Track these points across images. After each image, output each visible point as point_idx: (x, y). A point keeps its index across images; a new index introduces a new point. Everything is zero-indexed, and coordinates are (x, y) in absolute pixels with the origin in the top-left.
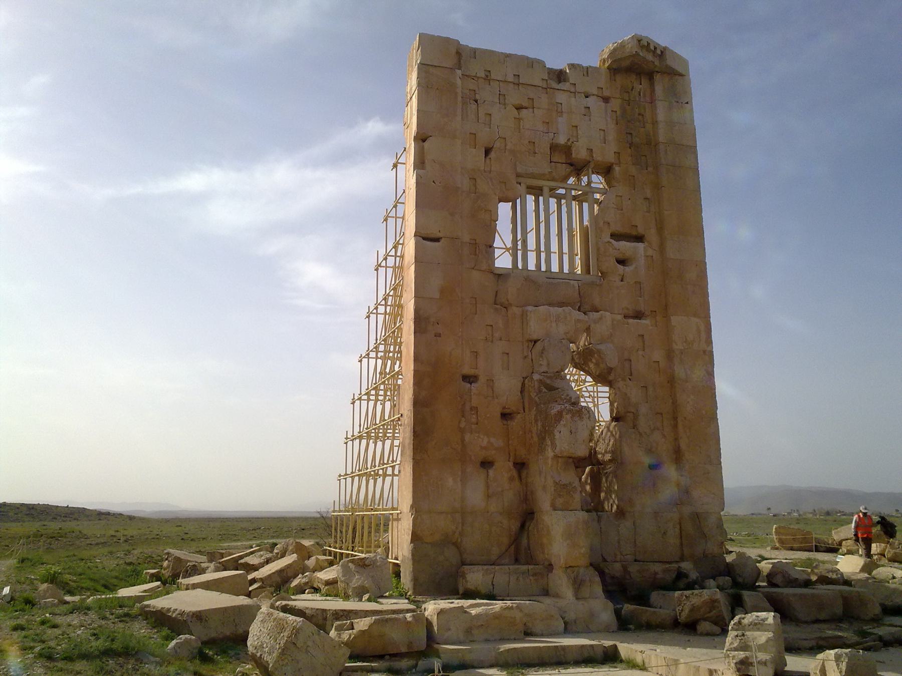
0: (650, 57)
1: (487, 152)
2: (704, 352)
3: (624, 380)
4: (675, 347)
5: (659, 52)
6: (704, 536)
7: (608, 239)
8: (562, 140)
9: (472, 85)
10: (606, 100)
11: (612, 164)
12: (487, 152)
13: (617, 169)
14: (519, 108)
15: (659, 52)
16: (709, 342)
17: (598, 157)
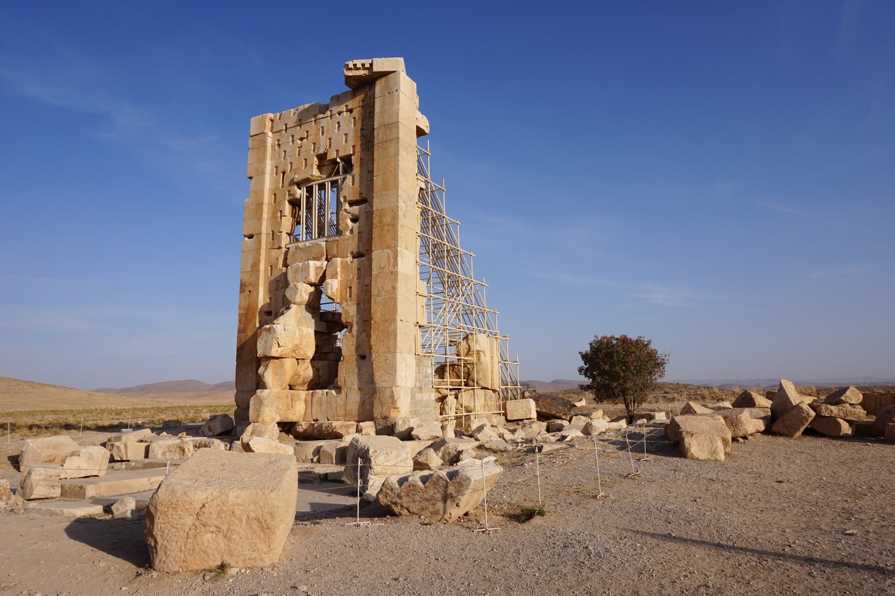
0: (362, 73)
1: (284, 173)
2: (392, 273)
3: (346, 301)
4: (373, 273)
5: (367, 66)
6: (382, 404)
7: (347, 206)
8: (322, 151)
9: (278, 136)
10: (351, 111)
11: (351, 155)
12: (284, 173)
13: (353, 157)
14: (301, 139)
15: (367, 66)
16: (396, 264)
17: (342, 154)
